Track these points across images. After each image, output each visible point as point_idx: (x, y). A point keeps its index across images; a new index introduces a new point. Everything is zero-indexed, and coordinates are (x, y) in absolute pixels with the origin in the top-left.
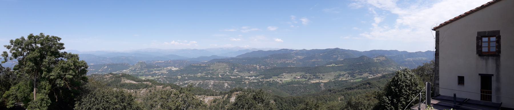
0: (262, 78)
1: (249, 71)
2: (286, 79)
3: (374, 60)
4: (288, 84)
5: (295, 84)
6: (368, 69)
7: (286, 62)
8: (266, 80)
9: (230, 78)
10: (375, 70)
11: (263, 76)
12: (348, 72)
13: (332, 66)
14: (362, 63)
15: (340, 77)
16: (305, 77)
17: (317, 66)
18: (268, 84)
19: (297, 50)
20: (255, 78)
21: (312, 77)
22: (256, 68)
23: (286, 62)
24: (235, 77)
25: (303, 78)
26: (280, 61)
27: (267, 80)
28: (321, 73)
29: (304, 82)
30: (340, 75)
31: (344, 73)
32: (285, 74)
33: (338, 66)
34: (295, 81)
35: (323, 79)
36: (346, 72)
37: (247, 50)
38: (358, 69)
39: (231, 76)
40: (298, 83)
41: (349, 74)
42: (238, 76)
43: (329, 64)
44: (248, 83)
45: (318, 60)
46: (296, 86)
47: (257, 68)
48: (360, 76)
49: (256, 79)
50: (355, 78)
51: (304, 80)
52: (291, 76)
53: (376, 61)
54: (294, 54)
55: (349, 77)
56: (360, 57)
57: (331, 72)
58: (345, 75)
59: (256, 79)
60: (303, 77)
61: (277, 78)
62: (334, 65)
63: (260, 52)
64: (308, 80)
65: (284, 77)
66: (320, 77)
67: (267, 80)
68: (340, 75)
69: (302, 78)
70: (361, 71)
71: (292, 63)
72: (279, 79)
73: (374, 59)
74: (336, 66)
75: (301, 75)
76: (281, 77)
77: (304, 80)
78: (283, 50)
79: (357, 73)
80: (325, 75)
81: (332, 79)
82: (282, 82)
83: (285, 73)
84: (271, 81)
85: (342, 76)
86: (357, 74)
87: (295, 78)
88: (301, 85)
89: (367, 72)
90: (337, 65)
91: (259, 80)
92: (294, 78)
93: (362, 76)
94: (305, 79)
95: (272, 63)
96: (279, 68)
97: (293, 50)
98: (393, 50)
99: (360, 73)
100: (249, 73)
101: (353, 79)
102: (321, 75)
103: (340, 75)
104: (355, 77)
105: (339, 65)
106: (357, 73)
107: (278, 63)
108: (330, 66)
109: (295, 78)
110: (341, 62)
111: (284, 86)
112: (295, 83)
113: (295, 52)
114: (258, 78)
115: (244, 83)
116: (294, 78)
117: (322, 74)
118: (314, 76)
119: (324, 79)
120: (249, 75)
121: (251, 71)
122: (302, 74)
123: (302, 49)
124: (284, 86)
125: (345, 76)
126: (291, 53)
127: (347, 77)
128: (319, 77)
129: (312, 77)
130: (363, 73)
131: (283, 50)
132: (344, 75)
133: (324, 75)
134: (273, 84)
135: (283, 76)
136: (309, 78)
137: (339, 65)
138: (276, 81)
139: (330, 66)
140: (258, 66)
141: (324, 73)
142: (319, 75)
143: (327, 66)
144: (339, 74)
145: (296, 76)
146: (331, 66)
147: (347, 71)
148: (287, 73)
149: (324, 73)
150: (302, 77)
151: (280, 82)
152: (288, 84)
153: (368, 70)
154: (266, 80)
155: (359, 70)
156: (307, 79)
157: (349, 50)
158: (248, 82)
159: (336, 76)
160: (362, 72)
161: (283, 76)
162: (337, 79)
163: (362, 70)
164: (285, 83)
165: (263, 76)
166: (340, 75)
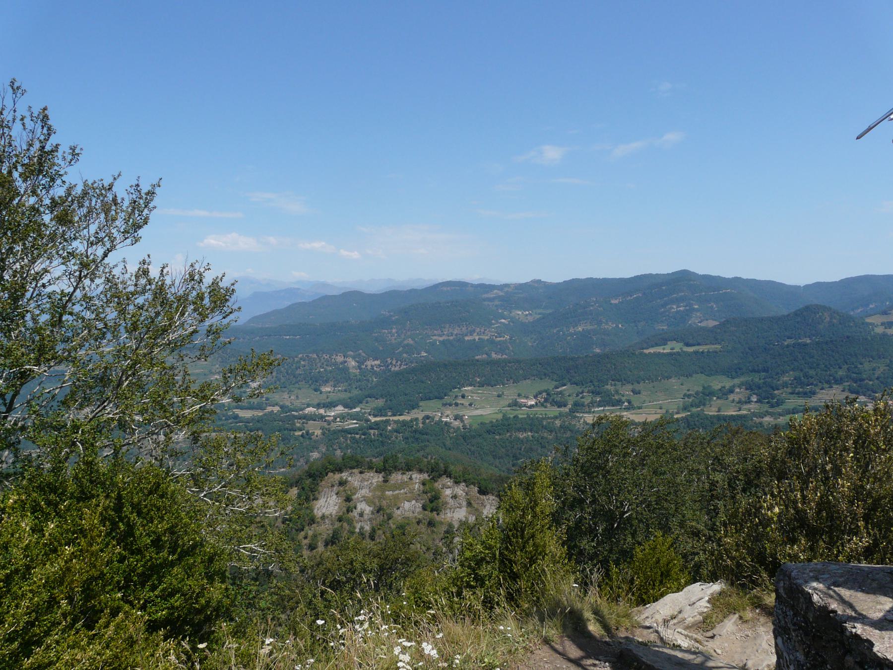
0: (379, 412)
1: (316, 382)
2: (477, 409)
3: (871, 324)
4: (489, 432)
5: (519, 430)
6: (846, 366)
7: (466, 338)
8: (396, 418)
9: (236, 417)
10: (878, 373)
11: (380, 402)
12: (743, 379)
13: (671, 354)
14: (808, 341)
15: (711, 400)
16: (558, 399)
17: (598, 350)
18: (407, 434)
19: (506, 285)
20: (348, 414)
21: (587, 401)
22: (345, 370)
23: (466, 338)
24: (260, 413)
25: (549, 405)
26: (439, 332)
27: (401, 418)
28: (625, 381)
29: (558, 423)
30: (711, 394)
31: (728, 383)
32: (470, 388)
33: (696, 353)
34: (516, 417)
35: (634, 408)
36: (737, 381)
37: (291, 291)
38: (793, 370)
39: (237, 408)
40: (533, 424)
41: (750, 387)
42: (269, 409)
43: (657, 345)
44: (323, 434)
45: (604, 326)
46: (527, 438)
47: (347, 369)
48: (801, 401)
49: (353, 417)
50: (779, 410)
51: (557, 414)
52: (499, 396)
53: (880, 330)
54: (497, 303)
55: (749, 401)
56: (796, 314)
57: (669, 378)
58: (731, 391)
59: (353, 417)
60: (550, 399)
61: (440, 406)
62: (678, 347)
63: (352, 297)
64: (572, 411)
65: (466, 403)
66: (624, 399)
67: (401, 418)
68: (708, 393)
69: (542, 405)
70: (806, 376)
71: (491, 342)
72: (449, 412)
73: (868, 320)
74: (688, 354)
75: (540, 393)
76: (457, 404)
77: (553, 411)
78: (445, 289)
79: (785, 385)
80: (643, 393)
81: (673, 408)
82: (462, 421)
83: (470, 385)
84: (417, 419)
85: (718, 398)
86: (789, 390)
87: (515, 404)
88: (545, 435)
89: (839, 381)
90: (691, 349)
91: (368, 420)
92: (509, 406)
93: (813, 402)
94: (559, 407)
95: (408, 345)
96: (445, 365)
97: (491, 287)
98: (750, 279)
99: (802, 384)
100: (316, 390)
101: (771, 414)
102: (626, 391)
103: (711, 394)
104: (778, 404)
105: (701, 348)
106: (785, 385)
107: (433, 344)
108: (660, 349)
109: (515, 404)
110: (712, 335)
111: (474, 437)
112: (519, 425)
113: (501, 294)
114: (358, 409)
115: (302, 436)
116: (509, 406)
117: (630, 387)
118: (597, 393)
119: (640, 408)
120: (316, 398)
121: (327, 381)
122: (543, 388)
123: (529, 280)
124: (474, 437)
125: (731, 397)
126: (484, 300)
127: (740, 402)
128: (617, 397)
129: (587, 401)
130: (816, 385)
131: (445, 289)
132: (725, 393)
133: (637, 389)
134: (427, 434)
135: (463, 397)
136: (576, 404)
137: (701, 348)
138: (437, 419)
139: (660, 349)
140: (354, 358)
141: (639, 383)
142: (617, 392)
143: (646, 351)
144: (704, 387)
145: (519, 395)
146: (667, 351)
147: (738, 376)
148: (481, 385)
149: (639, 383)
150: (546, 400)
151: (457, 423)
152: (489, 432)
153: (841, 373)
154: (396, 418)
155: (797, 374)
156: (565, 410)
157: (737, 279)
158: (318, 432)
159: (689, 396)
160: (811, 380)
161: (463, 397)
162: (694, 410)
163: (812, 372)
164: (475, 426)
165: (380, 402)
166: (708, 393)
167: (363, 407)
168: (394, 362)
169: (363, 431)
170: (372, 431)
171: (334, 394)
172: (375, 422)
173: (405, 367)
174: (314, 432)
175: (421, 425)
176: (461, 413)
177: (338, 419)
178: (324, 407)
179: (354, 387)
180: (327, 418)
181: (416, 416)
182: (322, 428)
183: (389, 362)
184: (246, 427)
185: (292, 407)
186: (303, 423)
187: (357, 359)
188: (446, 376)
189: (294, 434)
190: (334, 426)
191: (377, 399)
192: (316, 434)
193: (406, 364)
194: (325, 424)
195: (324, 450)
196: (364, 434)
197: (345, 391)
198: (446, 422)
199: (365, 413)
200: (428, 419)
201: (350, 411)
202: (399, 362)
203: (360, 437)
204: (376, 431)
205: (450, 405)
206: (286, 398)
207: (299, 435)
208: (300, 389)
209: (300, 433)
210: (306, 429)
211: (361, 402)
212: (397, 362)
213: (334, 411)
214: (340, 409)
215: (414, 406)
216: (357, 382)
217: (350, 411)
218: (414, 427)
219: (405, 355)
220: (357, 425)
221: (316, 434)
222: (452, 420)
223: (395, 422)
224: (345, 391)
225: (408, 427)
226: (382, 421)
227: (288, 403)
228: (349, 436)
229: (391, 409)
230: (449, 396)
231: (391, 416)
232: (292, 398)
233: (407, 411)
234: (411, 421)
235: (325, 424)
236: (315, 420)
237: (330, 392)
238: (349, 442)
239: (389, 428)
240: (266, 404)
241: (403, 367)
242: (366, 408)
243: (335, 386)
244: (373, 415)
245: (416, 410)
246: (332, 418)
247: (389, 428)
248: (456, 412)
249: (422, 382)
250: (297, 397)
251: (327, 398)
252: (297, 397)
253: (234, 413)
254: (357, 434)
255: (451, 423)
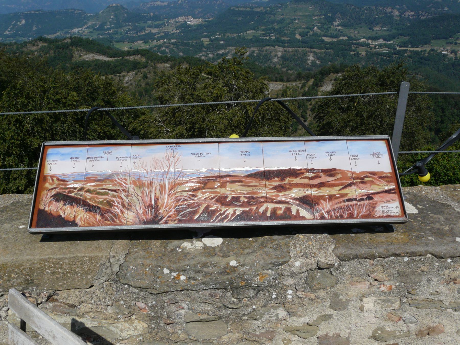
0: (404, 44)
8: (412, 49)
9: (323, 41)
11: (406, 39)
20: (385, 44)
22: (391, 17)
24: (335, 40)
27: (415, 49)
42: (342, 38)
44: (366, 54)
49: (386, 46)
59: (386, 46)
67: (415, 49)
76: (456, 43)
84: (425, 51)
91: (395, 49)
100: (370, 29)
114: (391, 42)
115: (354, 54)
134: (429, 60)
138: (439, 51)
140: (398, 10)
151: (452, 55)
154: (412, 49)
158: (364, 53)
165: (406, 39)
167: (395, 41)
168: (424, 13)
169: (389, 55)
170: (394, 56)
171: (380, 32)
172: (399, 50)
173: (430, 17)
174: (361, 53)
175: (426, 55)
176: (457, 49)
177: (377, 47)
178: (372, 39)
179: (394, 28)
180: (370, 46)
181: (426, 49)
182: (366, 51)
183: (421, 13)
184: (325, 47)
185: (354, 38)
186: (357, 47)
187: (401, 11)
188: (454, 24)
189: (350, 53)
190: (374, 51)
191: (405, 36)
192: (362, 54)
193: (432, 15)
194: (369, 49)
195: (364, 63)
196: (389, 57)
197: (388, 30)
198: (444, 54)
199: (395, 44)
200: (432, 51)
201: (386, 43)
202: (427, 14)
203: (386, 58)
204: (397, 56)
205: (451, 43)
206: (352, 33)
207: (353, 54)
208: (361, 27)
209: (353, 53)
210: (357, 51)
211: (394, 38)
212: (425, 14)
213: (377, 42)
214: (381, 41)
215: (427, 42)
216: (397, 25)
217: (386, 43)
218: (422, 55)
219: (433, 9)
220: (388, 51)
221: (362, 54)
222: (449, 53)
223: (410, 51)
224: (388, 30)
225: (418, 55)
226: (403, 50)
227: (352, 36)
228: (380, 57)
229: (411, 43)
230: (453, 37)
231: (410, 47)
232: (356, 32)
233: (421, 45)
234: (421, 51)
235: (369, 49)
236: (363, 46)
237: (378, 31)
238: (379, 61)
239: (406, 54)
240: (340, 35)
241: (429, 17)
242: (397, 41)
243: (382, 27)
244: (399, 46)
245: (427, 45)
246: (374, 46)
247: (406, 54)
248: (454, 48)
249: (437, 27)
250: (359, 32)
251: (376, 34)
252: (359, 32)
253: (322, 39)
254: (385, 56)
255: (448, 55)
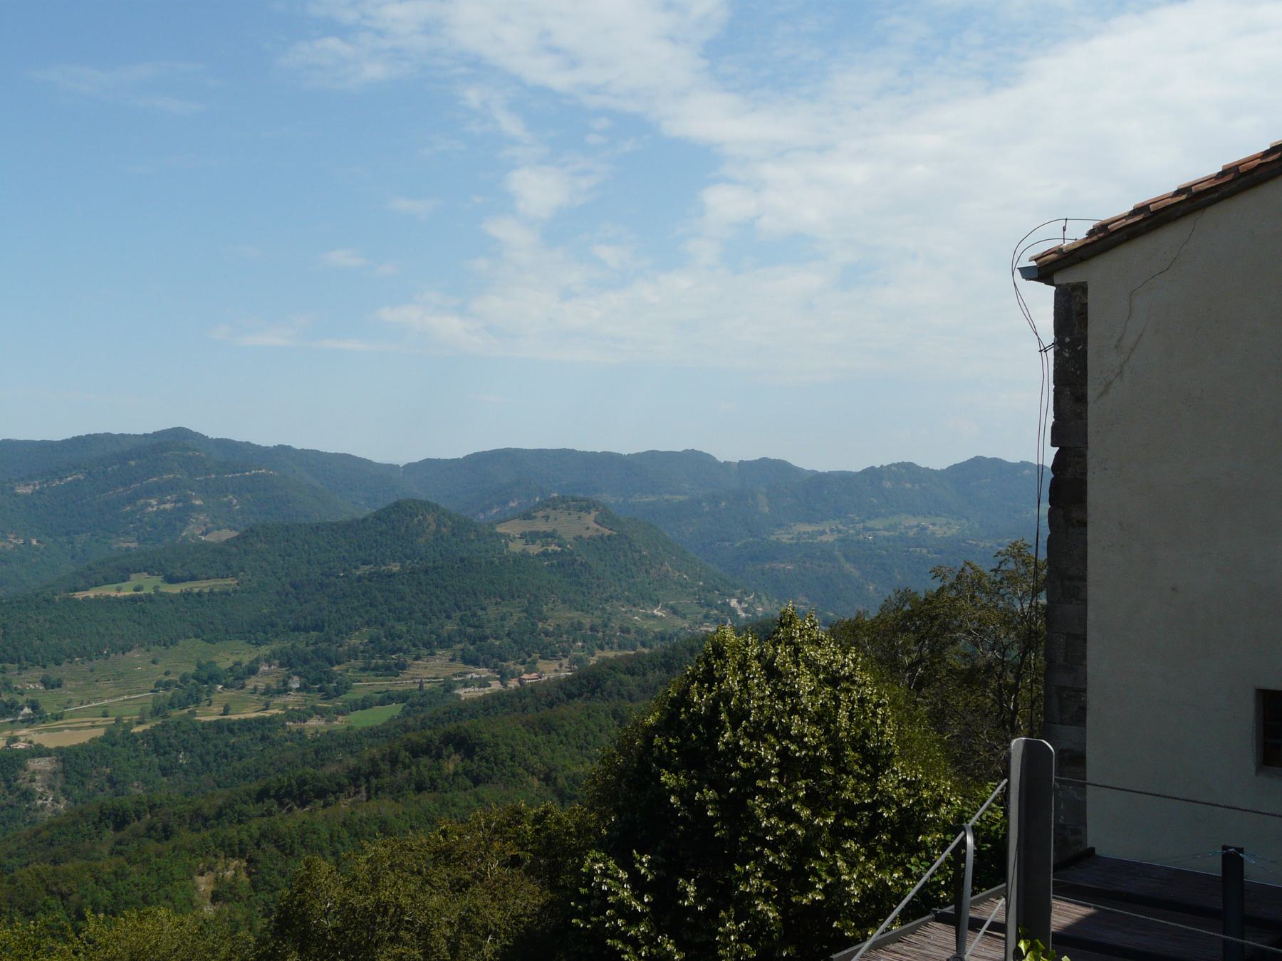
12: (276, 645)
13: (133, 600)
14: (395, 568)
15: (210, 692)
30: (214, 678)
31: (246, 655)
33: (186, 595)
35: (43, 719)
36: (264, 650)
38: (368, 624)
41: (287, 661)
55: (285, 690)
56: (378, 517)
57: (125, 649)
58: (252, 671)
62: (148, 584)
68: (208, 678)
70: (391, 635)
74: (171, 599)
79: (353, 654)
80: (69, 684)
81: (130, 714)
85: (226, 686)
90: (175, 589)
101: (321, 713)
103: (214, 678)
104: (338, 693)
105: (195, 586)
106: (353, 654)
119: (57, 718)
125: (251, 683)
127: (268, 692)
132: (239, 676)
137: (195, 586)
144: (200, 667)
147: (266, 641)
159: (167, 686)
160: (399, 643)
162: (176, 714)
163: (401, 627)
166: (208, 678)
